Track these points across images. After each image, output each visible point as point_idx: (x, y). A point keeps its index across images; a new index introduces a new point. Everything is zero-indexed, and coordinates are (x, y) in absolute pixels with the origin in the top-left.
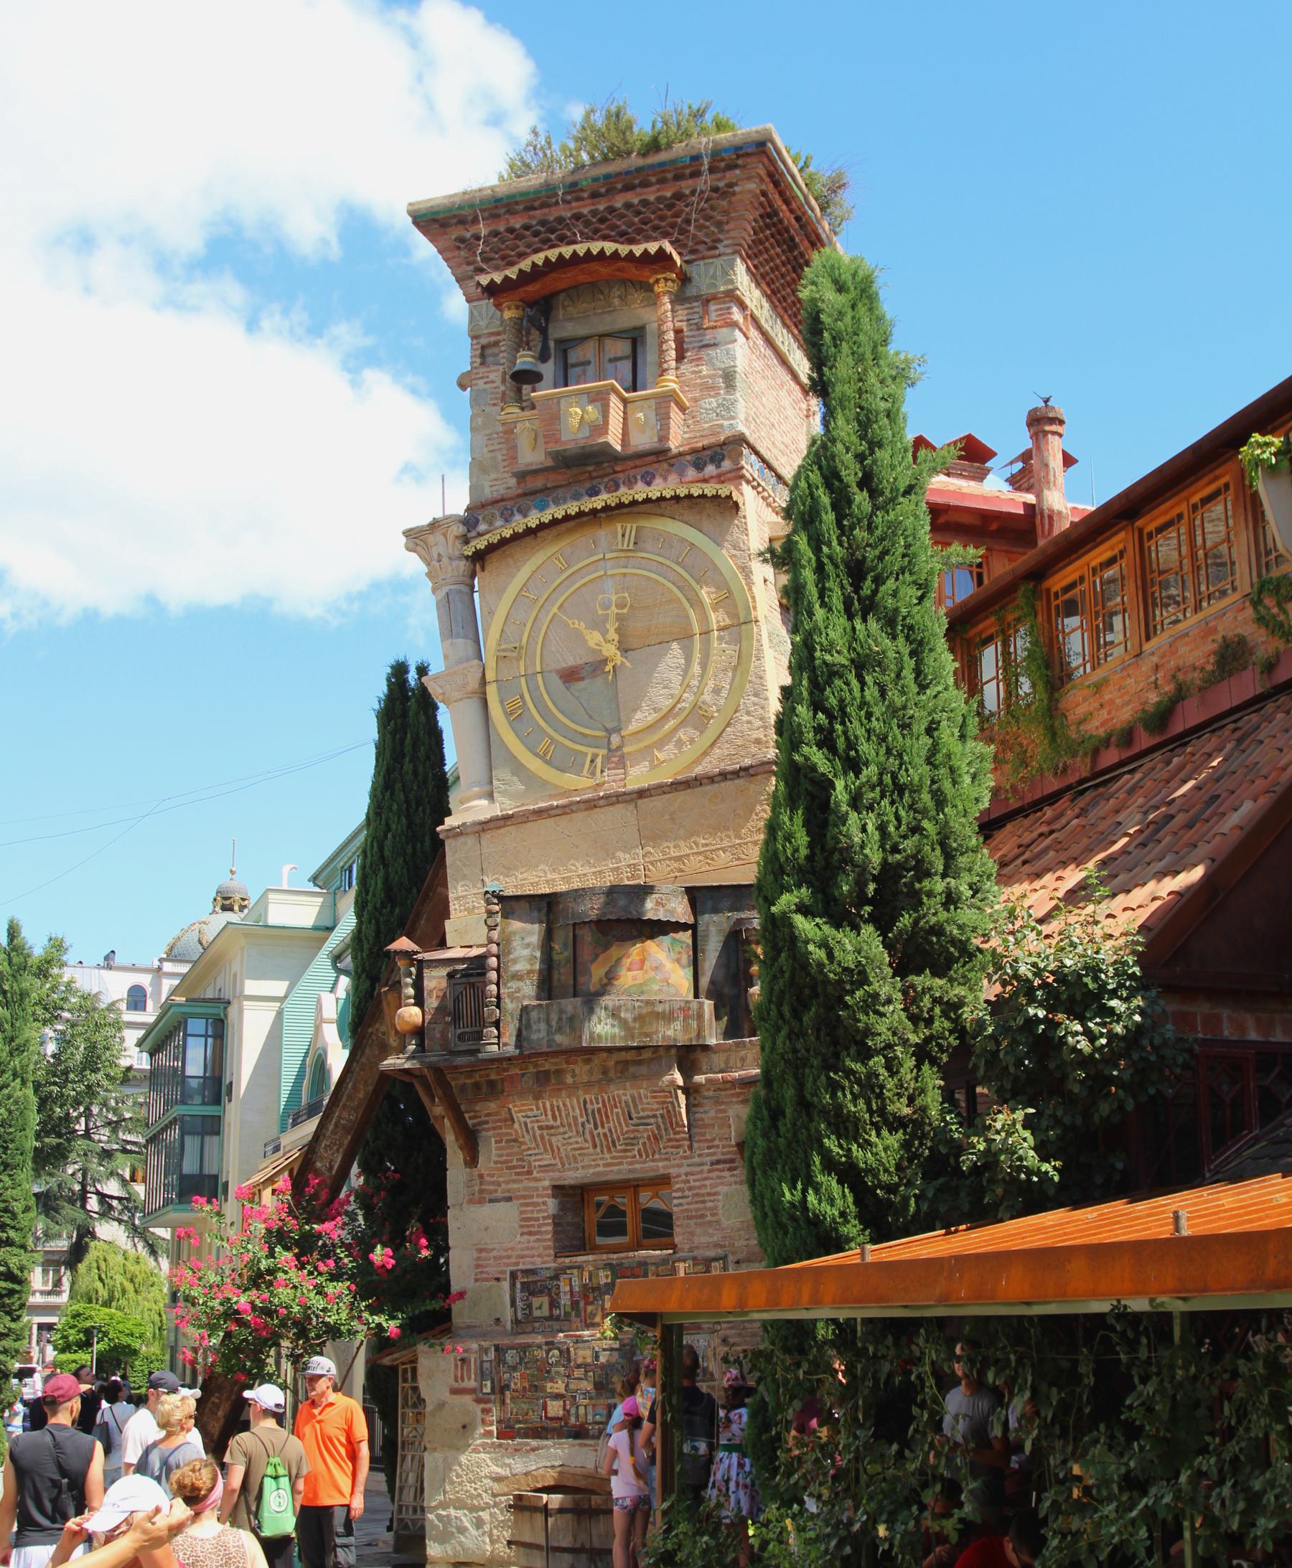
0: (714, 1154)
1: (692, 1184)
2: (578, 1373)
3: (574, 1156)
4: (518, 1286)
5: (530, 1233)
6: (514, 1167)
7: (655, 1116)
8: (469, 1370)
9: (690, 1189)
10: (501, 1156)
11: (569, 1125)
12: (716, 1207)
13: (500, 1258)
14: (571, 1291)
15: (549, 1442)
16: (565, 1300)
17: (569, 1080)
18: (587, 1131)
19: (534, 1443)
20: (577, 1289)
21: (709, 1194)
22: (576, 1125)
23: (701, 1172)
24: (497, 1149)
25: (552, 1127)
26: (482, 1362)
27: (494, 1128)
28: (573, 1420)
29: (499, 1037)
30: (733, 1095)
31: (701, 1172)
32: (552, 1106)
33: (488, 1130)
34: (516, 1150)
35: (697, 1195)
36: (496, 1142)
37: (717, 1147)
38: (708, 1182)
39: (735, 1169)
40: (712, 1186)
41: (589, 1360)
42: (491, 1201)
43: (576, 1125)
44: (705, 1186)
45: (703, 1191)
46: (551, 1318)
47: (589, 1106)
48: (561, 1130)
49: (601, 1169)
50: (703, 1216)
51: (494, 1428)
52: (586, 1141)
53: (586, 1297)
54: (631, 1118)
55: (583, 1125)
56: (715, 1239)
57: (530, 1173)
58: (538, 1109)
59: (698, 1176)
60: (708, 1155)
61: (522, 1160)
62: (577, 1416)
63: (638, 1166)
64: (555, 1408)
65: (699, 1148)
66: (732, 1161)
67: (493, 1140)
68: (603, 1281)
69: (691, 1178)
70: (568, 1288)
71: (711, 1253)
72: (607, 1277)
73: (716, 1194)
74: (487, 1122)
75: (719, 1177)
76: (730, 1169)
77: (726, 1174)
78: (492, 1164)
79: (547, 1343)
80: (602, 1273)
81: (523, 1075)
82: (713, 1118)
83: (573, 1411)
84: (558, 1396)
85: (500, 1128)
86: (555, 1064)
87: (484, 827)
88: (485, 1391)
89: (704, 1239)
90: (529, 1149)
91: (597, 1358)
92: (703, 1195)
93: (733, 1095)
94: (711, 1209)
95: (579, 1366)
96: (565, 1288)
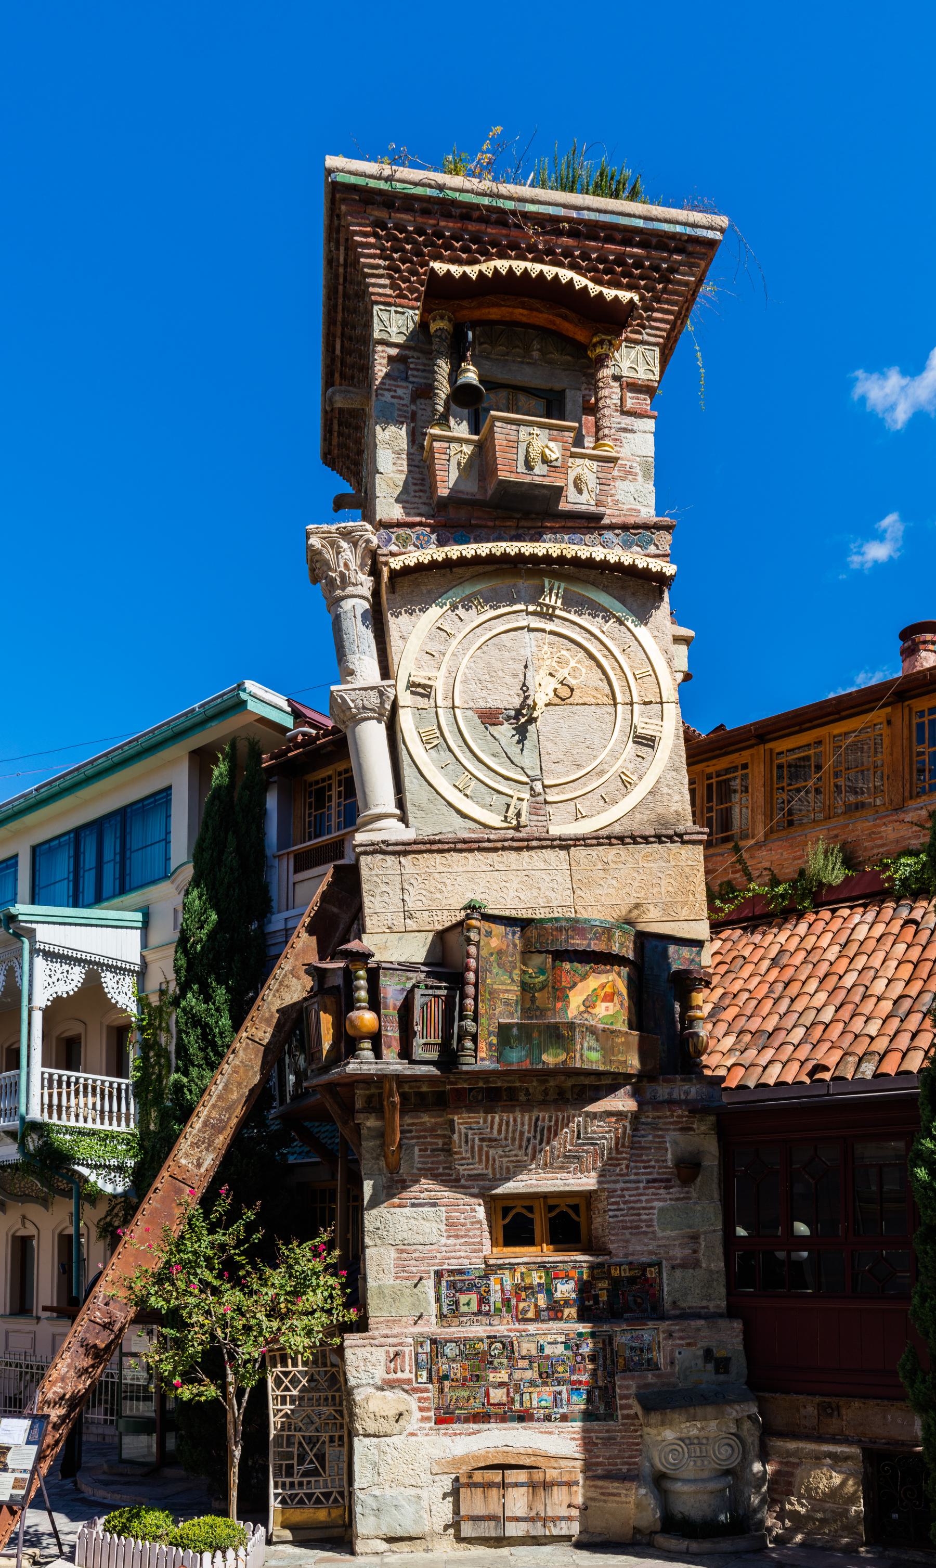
0: (650, 1173)
1: (627, 1198)
2: (522, 1364)
3: (508, 1168)
4: (444, 1284)
5: (457, 1237)
6: (441, 1175)
7: (605, 1138)
8: (403, 1362)
9: (625, 1203)
10: (426, 1163)
11: (514, 1139)
12: (651, 1220)
13: (423, 1259)
14: (502, 1290)
15: (493, 1425)
16: (495, 1297)
17: (523, 1098)
18: (530, 1147)
19: (475, 1426)
20: (509, 1288)
21: (644, 1208)
22: (521, 1139)
23: (638, 1188)
24: (420, 1156)
25: (496, 1140)
26: (417, 1354)
27: (418, 1138)
28: (517, 1406)
29: (476, 1051)
30: (671, 1123)
31: (638, 1188)
32: (501, 1120)
33: (412, 1138)
34: (442, 1158)
35: (633, 1208)
36: (420, 1150)
37: (654, 1167)
38: (643, 1198)
39: (671, 1187)
40: (647, 1201)
41: (534, 1352)
42: (413, 1205)
43: (521, 1139)
44: (640, 1201)
45: (639, 1205)
46: (480, 1312)
47: (539, 1123)
48: (504, 1143)
49: (534, 1182)
50: (638, 1227)
51: (432, 1414)
52: (526, 1155)
53: (517, 1295)
54: (579, 1137)
55: (529, 1140)
56: (651, 1248)
57: (458, 1180)
58: (485, 1122)
59: (635, 1192)
60: (643, 1174)
61: (450, 1168)
62: (522, 1404)
63: (571, 1181)
64: (498, 1395)
65: (636, 1167)
66: (668, 1180)
67: (417, 1149)
68: (536, 1281)
69: (626, 1193)
70: (499, 1287)
71: (644, 1259)
72: (540, 1277)
73: (652, 1208)
74: (410, 1131)
75: (653, 1194)
76: (665, 1188)
77: (662, 1191)
78: (415, 1171)
79: (489, 1337)
80: (535, 1275)
81: (471, 1090)
82: (651, 1142)
83: (517, 1397)
84: (501, 1385)
85: (426, 1137)
86: (508, 1082)
87: (403, 850)
88: (420, 1380)
89: (638, 1248)
90: (463, 1158)
91: (541, 1348)
92: (639, 1209)
93: (671, 1123)
94: (645, 1221)
95: (523, 1358)
96: (495, 1286)
